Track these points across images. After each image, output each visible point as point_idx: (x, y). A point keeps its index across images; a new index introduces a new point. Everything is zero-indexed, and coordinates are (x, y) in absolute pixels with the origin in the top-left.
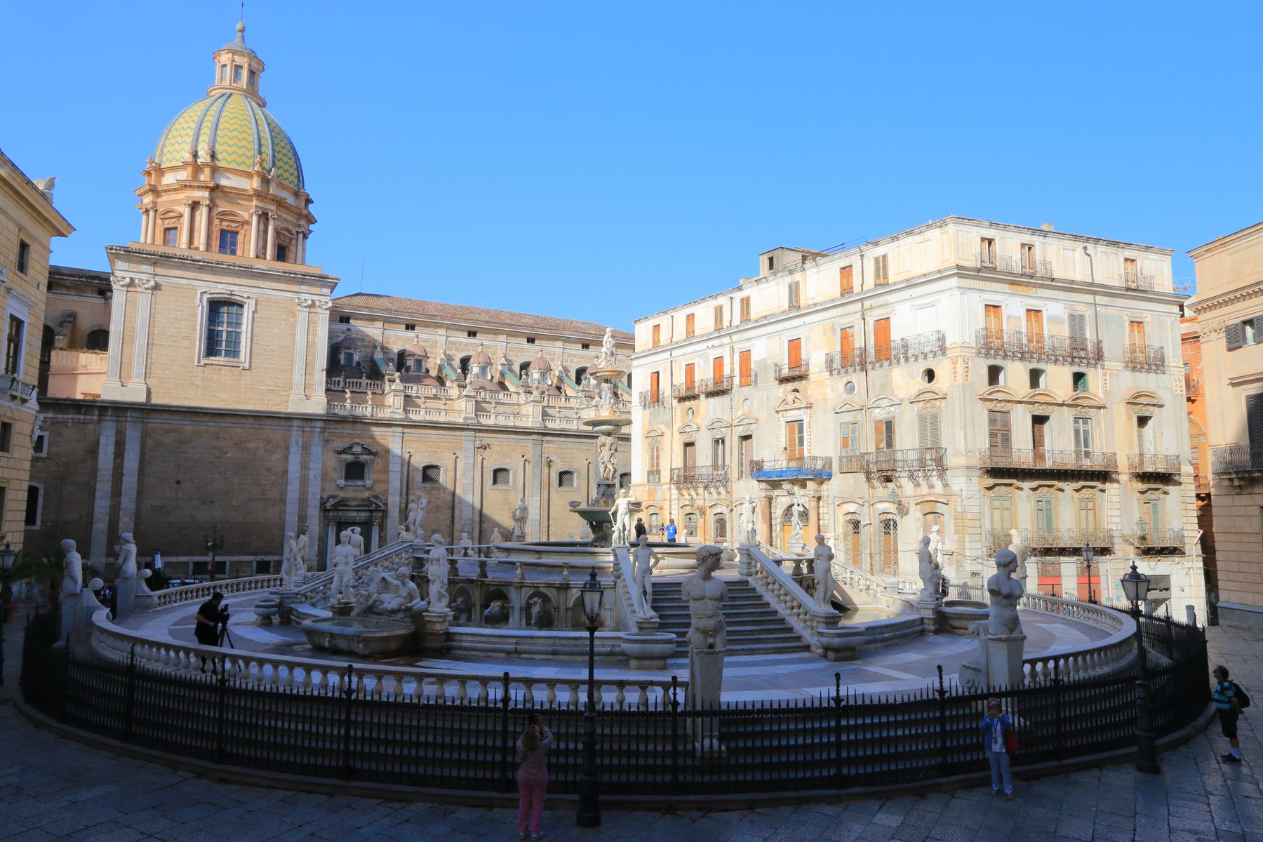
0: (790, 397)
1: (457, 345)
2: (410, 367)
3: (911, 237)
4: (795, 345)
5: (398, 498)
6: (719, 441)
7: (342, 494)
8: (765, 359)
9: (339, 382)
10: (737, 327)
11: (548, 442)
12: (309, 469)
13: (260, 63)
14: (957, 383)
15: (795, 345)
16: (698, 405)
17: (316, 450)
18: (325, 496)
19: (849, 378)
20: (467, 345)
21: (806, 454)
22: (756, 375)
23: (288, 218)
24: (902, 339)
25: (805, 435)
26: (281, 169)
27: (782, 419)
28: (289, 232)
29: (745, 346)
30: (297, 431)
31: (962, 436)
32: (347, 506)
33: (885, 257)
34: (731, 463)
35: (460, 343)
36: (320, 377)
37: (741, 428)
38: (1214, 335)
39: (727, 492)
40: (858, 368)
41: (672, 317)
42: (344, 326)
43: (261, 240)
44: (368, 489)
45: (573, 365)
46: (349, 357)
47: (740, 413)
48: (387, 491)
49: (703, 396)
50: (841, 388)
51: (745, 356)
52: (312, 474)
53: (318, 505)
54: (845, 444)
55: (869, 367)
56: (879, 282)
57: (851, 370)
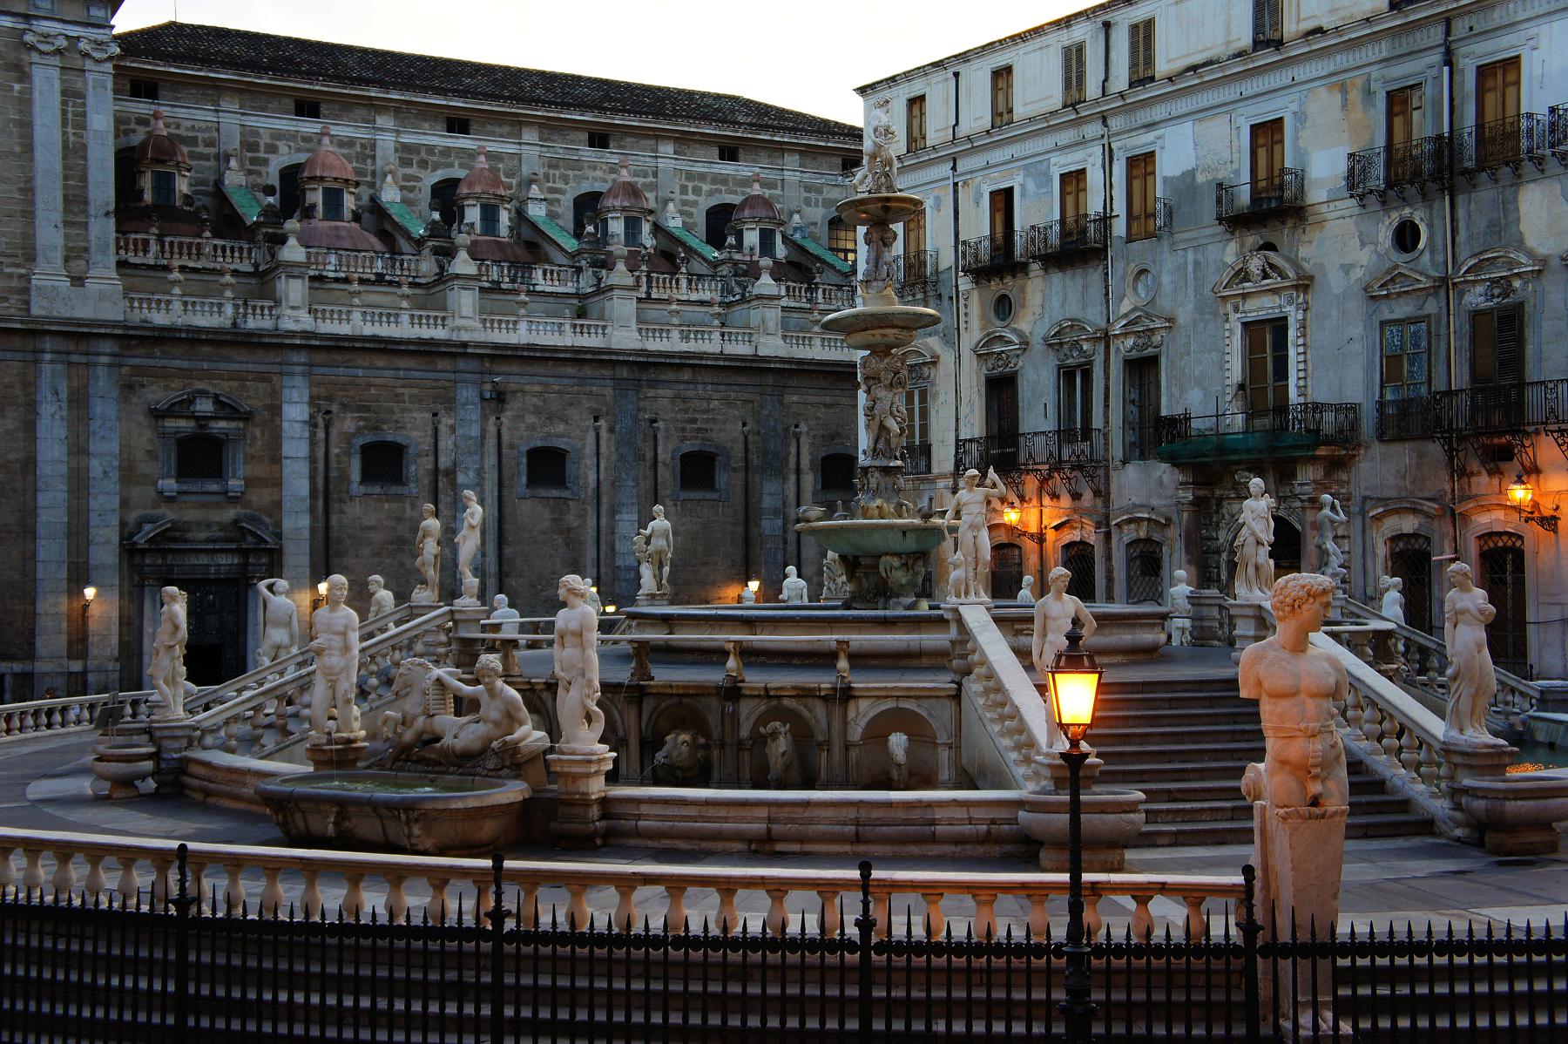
0: (1255, 265)
1: (423, 154)
2: (314, 206)
4: (1267, 134)
5: (305, 521)
6: (1074, 377)
7: (170, 514)
8: (1192, 173)
9: (146, 243)
10: (1122, 95)
11: (653, 384)
12: (88, 454)
15: (1267, 134)
16: (1023, 290)
17: (104, 408)
18: (133, 516)
20: (447, 151)
21: (1293, 396)
22: (1170, 214)
24: (1552, 110)
25: (1292, 352)
27: (1234, 317)
29: (1140, 142)
30: (52, 362)
32: (186, 541)
34: (1107, 422)
35: (430, 149)
36: (103, 229)
37: (1130, 342)
39: (1097, 493)
40: (1431, 186)
41: (956, 75)
42: (142, 107)
44: (234, 500)
45: (701, 199)
46: (164, 184)
47: (1126, 306)
48: (278, 505)
49: (1035, 267)
50: (1384, 234)
51: (1141, 164)
52: (96, 466)
53: (116, 539)
55: (1460, 180)
57: (1411, 191)
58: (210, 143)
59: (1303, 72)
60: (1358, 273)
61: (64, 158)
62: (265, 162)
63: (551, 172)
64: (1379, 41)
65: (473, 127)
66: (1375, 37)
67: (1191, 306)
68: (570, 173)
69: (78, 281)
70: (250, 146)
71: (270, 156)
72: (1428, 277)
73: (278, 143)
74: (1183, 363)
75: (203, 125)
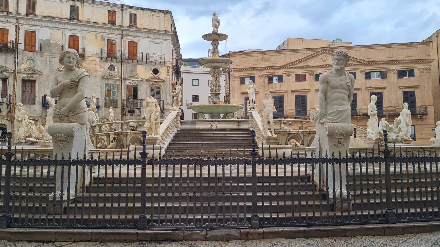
3: (150, 12)
8: (49, 40)
14: (169, 77)
19: (112, 63)
31: (170, 98)
33: (135, 15)
37: (25, 75)
38: (236, 79)
47: (23, 67)
54: (108, 93)
56: (131, 25)
57: (114, 59)
59: (84, 28)
60: (99, 73)
64: (106, 29)
66: (105, 28)
67: (48, 70)
72: (119, 77)
74: (45, 83)
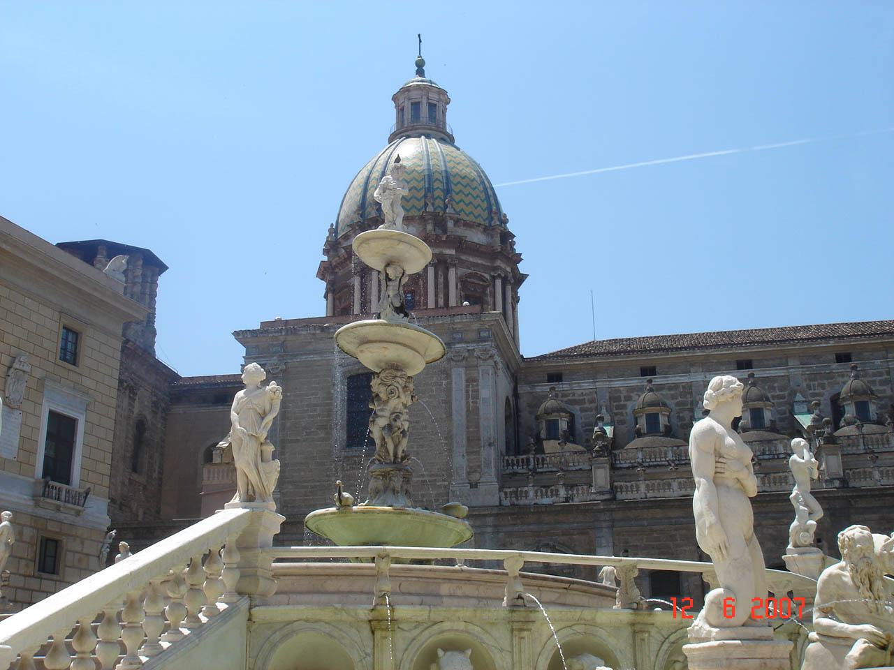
9: (528, 460)
13: (442, 92)
23: (480, 262)
26: (462, 203)
28: (482, 278)
36: (490, 455)
43: (441, 295)
58: (592, 401)
61: (467, 416)
62: (624, 407)
63: (812, 383)
65: (755, 363)
68: (826, 382)
69: (474, 485)
70: (618, 399)
71: (628, 403)
73: (632, 394)
75: (587, 391)
